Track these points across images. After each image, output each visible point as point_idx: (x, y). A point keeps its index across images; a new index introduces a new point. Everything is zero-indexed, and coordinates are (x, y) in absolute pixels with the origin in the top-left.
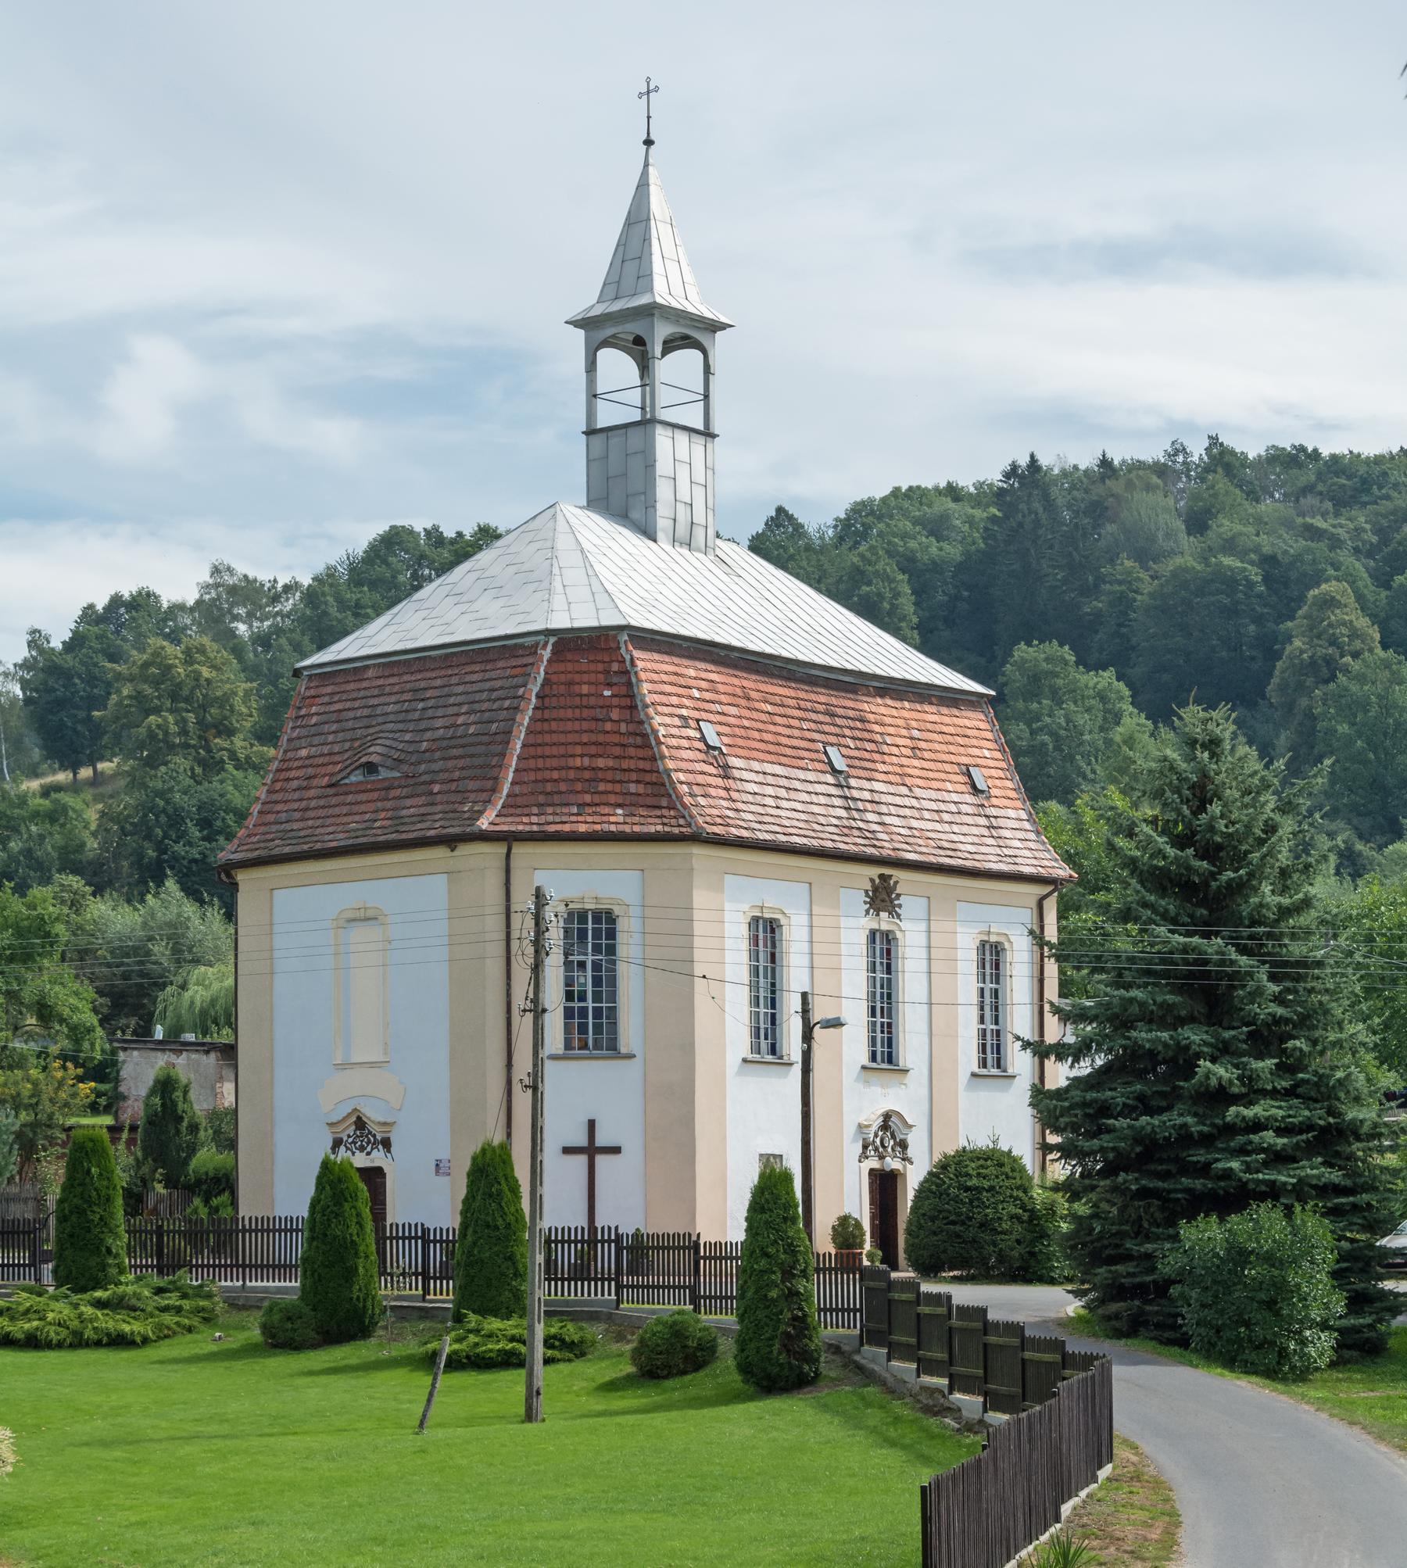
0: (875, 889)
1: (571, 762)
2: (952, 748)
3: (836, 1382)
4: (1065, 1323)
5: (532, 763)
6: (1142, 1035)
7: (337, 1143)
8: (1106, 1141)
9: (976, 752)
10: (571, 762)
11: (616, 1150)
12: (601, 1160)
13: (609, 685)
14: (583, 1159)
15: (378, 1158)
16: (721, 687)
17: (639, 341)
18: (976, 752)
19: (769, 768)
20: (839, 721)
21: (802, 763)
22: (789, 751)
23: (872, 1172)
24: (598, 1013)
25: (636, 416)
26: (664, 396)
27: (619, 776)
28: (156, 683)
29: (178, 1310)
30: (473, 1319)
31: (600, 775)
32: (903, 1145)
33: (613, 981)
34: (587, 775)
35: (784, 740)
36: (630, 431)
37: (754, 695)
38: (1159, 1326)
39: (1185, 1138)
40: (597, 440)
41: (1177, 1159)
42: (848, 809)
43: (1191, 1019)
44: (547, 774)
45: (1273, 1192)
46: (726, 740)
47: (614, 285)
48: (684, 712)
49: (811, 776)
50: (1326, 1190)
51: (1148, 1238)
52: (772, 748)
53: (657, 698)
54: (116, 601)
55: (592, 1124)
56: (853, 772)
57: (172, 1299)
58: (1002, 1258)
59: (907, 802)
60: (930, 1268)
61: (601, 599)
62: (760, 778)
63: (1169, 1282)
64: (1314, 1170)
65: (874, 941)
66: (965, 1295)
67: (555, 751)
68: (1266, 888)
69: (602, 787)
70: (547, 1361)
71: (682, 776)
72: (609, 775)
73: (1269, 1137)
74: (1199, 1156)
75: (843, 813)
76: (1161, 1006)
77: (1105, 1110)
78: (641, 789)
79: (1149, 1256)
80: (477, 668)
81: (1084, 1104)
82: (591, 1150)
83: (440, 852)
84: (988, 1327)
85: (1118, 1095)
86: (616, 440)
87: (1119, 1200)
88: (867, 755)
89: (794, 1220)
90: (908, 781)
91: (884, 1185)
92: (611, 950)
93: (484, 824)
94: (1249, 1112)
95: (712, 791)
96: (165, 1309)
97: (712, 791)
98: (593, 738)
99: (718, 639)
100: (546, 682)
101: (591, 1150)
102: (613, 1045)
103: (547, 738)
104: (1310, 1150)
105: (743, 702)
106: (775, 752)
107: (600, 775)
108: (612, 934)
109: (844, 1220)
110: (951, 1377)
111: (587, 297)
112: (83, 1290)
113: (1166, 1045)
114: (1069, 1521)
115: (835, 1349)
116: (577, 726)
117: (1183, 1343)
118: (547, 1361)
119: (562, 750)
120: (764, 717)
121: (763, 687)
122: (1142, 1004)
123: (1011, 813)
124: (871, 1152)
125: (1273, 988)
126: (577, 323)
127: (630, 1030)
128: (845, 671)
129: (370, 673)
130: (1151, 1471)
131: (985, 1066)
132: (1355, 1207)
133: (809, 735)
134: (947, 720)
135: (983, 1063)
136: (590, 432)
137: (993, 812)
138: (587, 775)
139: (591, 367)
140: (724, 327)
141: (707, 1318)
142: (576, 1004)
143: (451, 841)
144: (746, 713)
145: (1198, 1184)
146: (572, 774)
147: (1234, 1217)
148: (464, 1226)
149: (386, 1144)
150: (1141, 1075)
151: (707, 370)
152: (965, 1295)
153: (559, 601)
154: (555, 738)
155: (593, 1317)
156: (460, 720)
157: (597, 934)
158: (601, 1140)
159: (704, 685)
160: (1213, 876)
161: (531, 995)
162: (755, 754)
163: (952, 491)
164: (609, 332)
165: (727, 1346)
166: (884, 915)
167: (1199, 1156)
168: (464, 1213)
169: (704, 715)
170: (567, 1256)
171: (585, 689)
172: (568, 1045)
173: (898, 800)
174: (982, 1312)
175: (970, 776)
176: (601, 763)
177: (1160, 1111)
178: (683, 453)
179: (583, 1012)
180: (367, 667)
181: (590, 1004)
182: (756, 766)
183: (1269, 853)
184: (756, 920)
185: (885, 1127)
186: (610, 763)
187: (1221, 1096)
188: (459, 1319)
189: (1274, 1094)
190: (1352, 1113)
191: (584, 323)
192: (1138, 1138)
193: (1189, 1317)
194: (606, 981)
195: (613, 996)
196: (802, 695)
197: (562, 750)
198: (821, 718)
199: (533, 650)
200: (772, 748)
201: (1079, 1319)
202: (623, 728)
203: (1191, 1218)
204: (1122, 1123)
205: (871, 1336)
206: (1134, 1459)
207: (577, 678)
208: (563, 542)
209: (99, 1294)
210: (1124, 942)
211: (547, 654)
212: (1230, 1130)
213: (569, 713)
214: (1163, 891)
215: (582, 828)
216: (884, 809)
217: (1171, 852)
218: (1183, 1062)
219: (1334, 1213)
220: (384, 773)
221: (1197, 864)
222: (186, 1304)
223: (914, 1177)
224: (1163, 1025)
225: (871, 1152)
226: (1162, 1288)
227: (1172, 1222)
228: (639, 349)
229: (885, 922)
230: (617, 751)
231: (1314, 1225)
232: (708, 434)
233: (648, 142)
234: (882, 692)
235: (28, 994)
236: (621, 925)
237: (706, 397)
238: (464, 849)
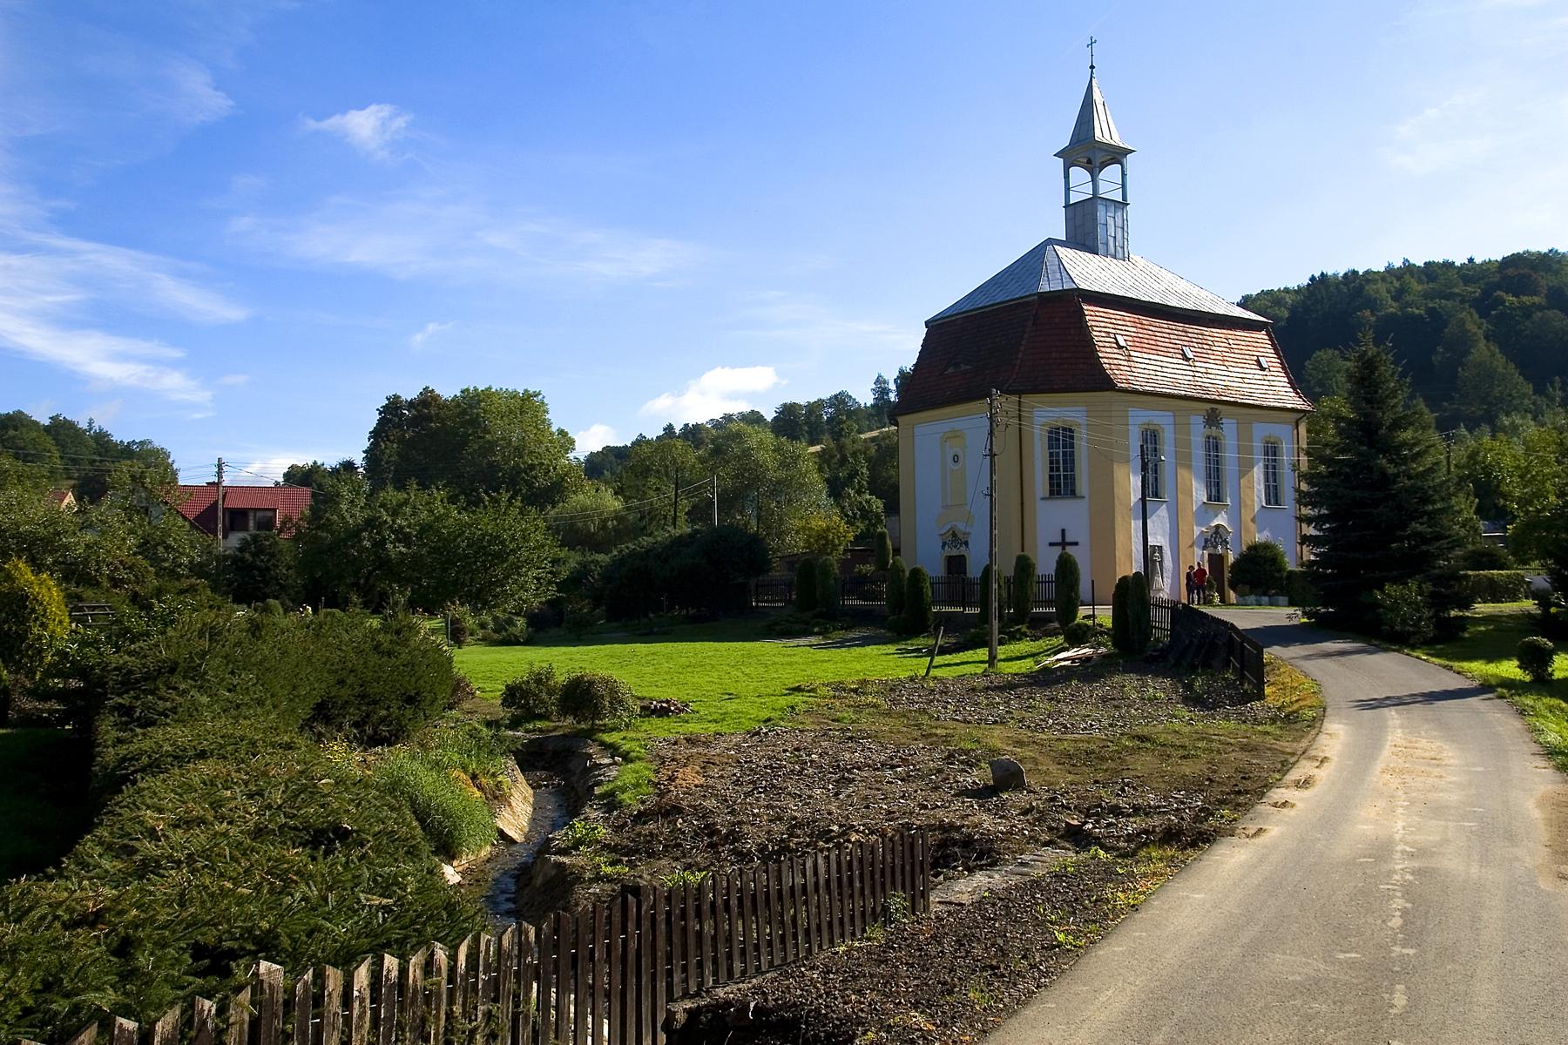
7: (944, 544)
16: (1127, 319)
21: (1170, 355)
33: (1073, 461)
36: (1085, 203)
46: (1129, 343)
53: (1094, 323)
55: (1063, 531)
56: (1196, 359)
71: (1106, 361)
90: (1226, 363)
95: (1122, 368)
97: (1122, 368)
105: (1139, 326)
127: (1082, 485)
131: (1270, 504)
135: (1268, 502)
149: (966, 543)
156: (998, 340)
158: (1068, 539)
161: (988, 447)
162: (1145, 350)
163: (1287, 290)
169: (1118, 332)
172: (1051, 493)
176: (1065, 355)
182: (1145, 356)
198: (1180, 333)
229: (1214, 431)
233: (1092, 67)
237: (1124, 186)
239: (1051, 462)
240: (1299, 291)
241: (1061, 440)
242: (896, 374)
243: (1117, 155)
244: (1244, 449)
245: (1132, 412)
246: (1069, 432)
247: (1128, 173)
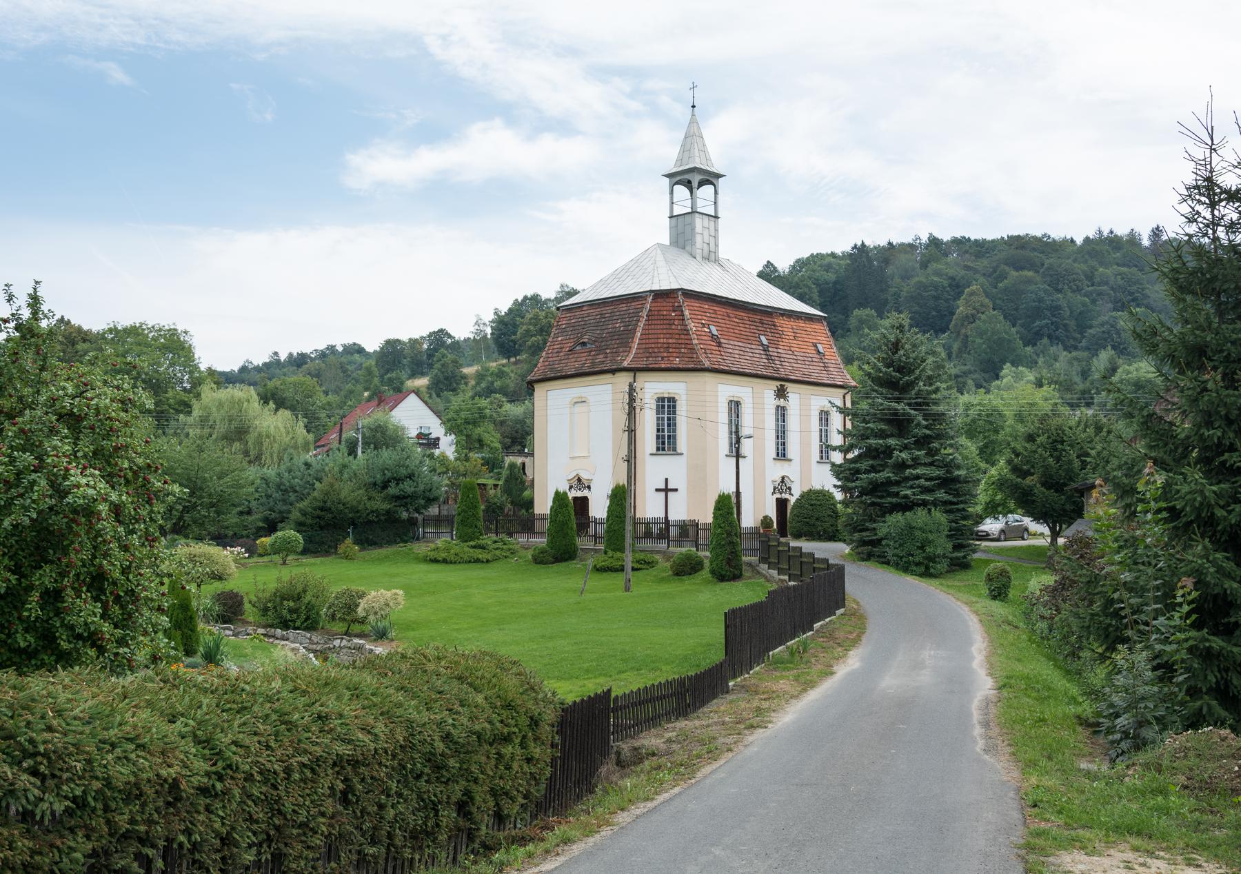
0: (778, 390)
3: (750, 578)
4: (843, 557)
6: (872, 441)
8: (858, 483)
11: (676, 490)
12: (670, 494)
13: (674, 311)
14: (663, 494)
15: (586, 493)
17: (689, 182)
19: (736, 343)
23: (777, 499)
24: (669, 437)
25: (690, 210)
26: (700, 203)
27: (678, 346)
28: (535, 325)
29: (502, 549)
30: (610, 553)
32: (790, 489)
33: (675, 425)
38: (878, 556)
39: (889, 482)
41: (886, 491)
43: (892, 436)
45: (924, 504)
47: (680, 160)
49: (753, 347)
50: (945, 503)
51: (875, 522)
54: (526, 298)
55: (667, 480)
57: (500, 545)
58: (825, 531)
60: (797, 536)
63: (882, 539)
64: (941, 495)
66: (794, 544)
68: (921, 383)
70: (633, 569)
73: (922, 481)
74: (895, 489)
76: (881, 430)
77: (858, 471)
78: (686, 351)
79: (874, 529)
81: (850, 469)
82: (666, 490)
83: (609, 376)
84: (802, 554)
85: (863, 465)
86: (680, 219)
87: (863, 506)
89: (732, 514)
91: (781, 504)
92: (674, 413)
93: (625, 364)
94: (914, 472)
96: (497, 549)
100: (650, 310)
101: (666, 490)
102: (675, 449)
104: (940, 486)
106: (740, 339)
108: (674, 407)
109: (766, 517)
110: (790, 575)
112: (466, 541)
113: (881, 445)
114: (817, 631)
115: (750, 564)
117: (888, 563)
118: (633, 569)
122: (872, 429)
124: (777, 491)
125: (924, 423)
126: (666, 176)
128: (768, 307)
129: (585, 308)
130: (862, 612)
132: (958, 510)
135: (822, 458)
139: (672, 192)
140: (722, 176)
141: (700, 553)
142: (661, 434)
143: (613, 372)
145: (894, 500)
147: (908, 513)
148: (608, 517)
149: (589, 487)
150: (874, 458)
151: (716, 193)
152: (807, 546)
153: (656, 280)
155: (658, 552)
157: (669, 407)
160: (901, 379)
163: (833, 255)
164: (678, 178)
165: (707, 563)
166: (782, 400)
167: (895, 489)
168: (608, 512)
170: (655, 530)
172: (658, 449)
174: (801, 548)
175: (816, 346)
176: (670, 341)
177: (879, 471)
178: (706, 224)
179: (664, 436)
181: (666, 434)
182: (732, 342)
183: (923, 370)
185: (782, 482)
186: (674, 341)
187: (902, 466)
188: (606, 553)
189: (925, 465)
190: (957, 473)
191: (669, 176)
192: (871, 483)
193: (890, 553)
194: (672, 424)
195: (675, 431)
199: (645, 298)
201: (849, 554)
203: (891, 513)
204: (865, 476)
205: (764, 560)
206: (856, 607)
209: (471, 543)
210: (864, 406)
211: (650, 299)
212: (907, 479)
213: (658, 322)
214: (881, 385)
215: (663, 366)
217: (884, 369)
218: (888, 452)
219: (946, 512)
221: (894, 374)
222: (505, 547)
223: (793, 500)
224: (881, 437)
225: (777, 491)
226: (879, 541)
227: (883, 515)
228: (688, 184)
229: (782, 402)
230: (677, 336)
231: (939, 516)
232: (716, 217)
233: (693, 107)
234: (783, 315)
235: (475, 437)
236: (678, 403)
238: (618, 375)
239: (658, 425)
240: (846, 256)
242: (492, 317)
243: (710, 178)
244: (804, 415)
245: (721, 387)
246: (672, 401)
247: (720, 191)
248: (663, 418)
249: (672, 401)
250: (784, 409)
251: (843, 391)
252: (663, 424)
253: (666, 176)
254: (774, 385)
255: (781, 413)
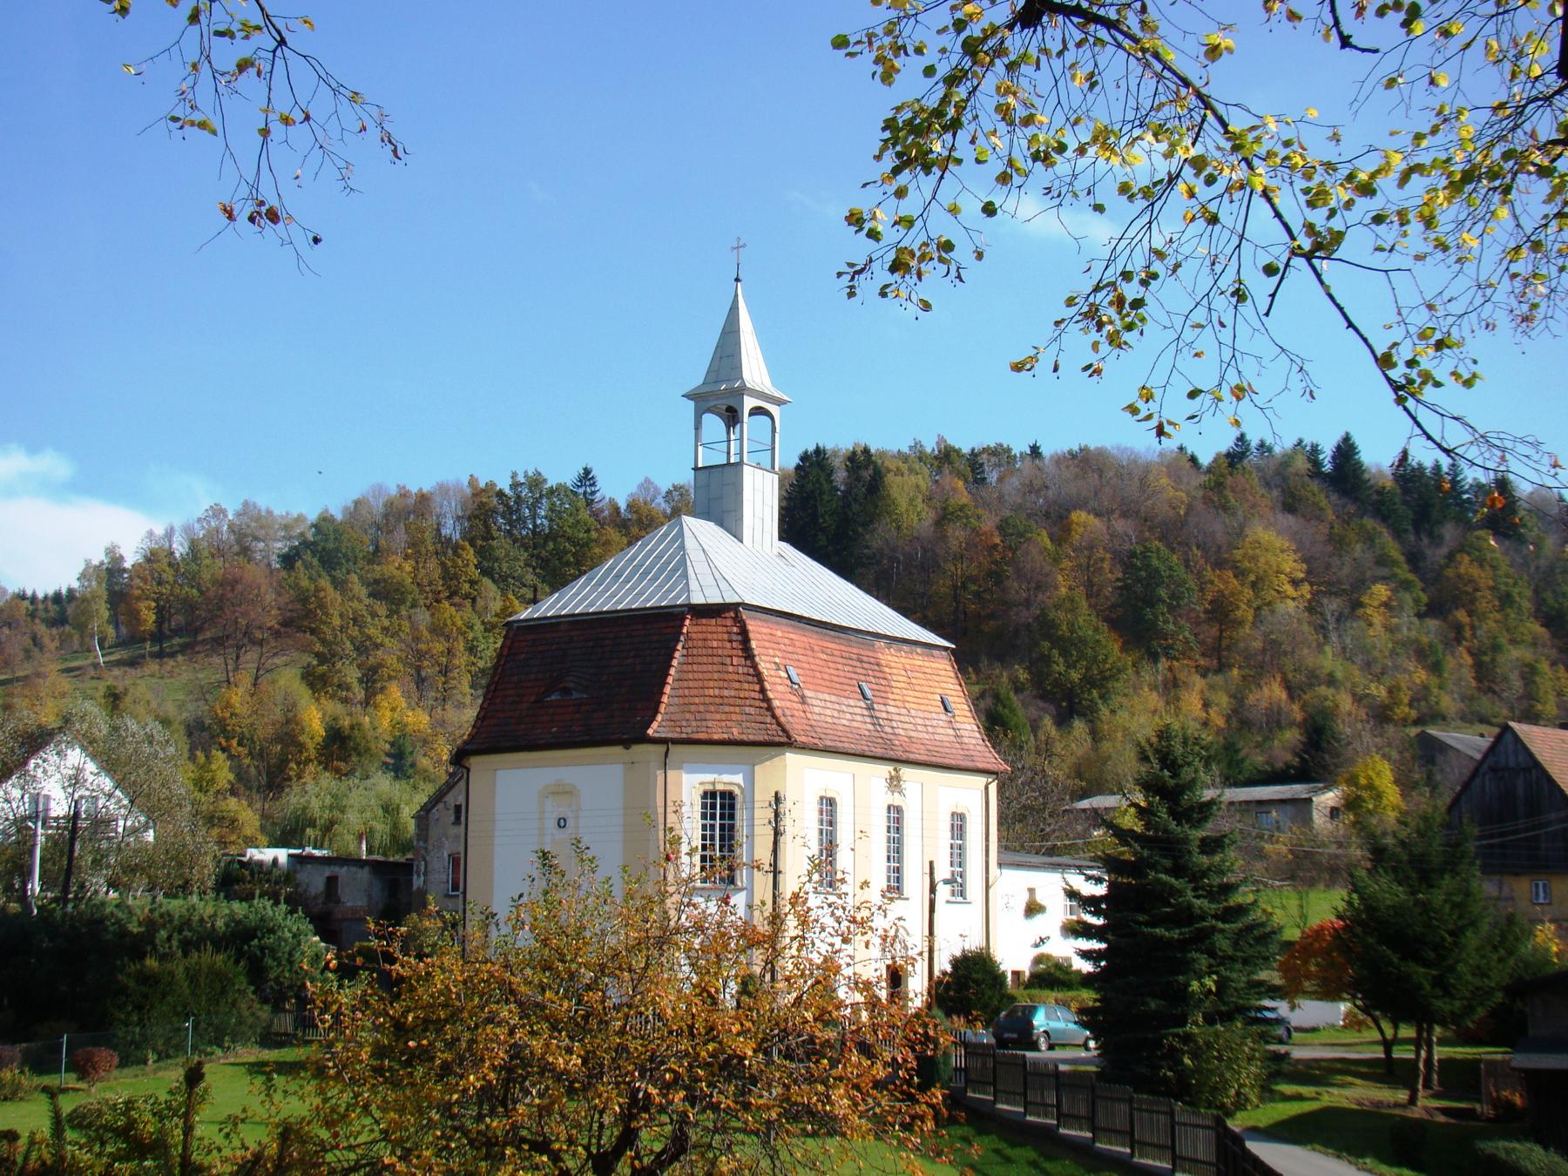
0: (891, 778)
1: (707, 692)
2: (931, 683)
5: (681, 692)
9: (945, 685)
10: (707, 692)
18: (945, 685)
20: (866, 665)
21: (846, 694)
22: (838, 686)
27: (739, 702)
31: (726, 700)
34: (718, 701)
35: (836, 679)
37: (816, 648)
40: (699, 472)
42: (874, 724)
44: (692, 700)
48: (777, 660)
49: (852, 702)
52: (828, 683)
56: (875, 700)
59: (907, 719)
61: (723, 584)
62: (823, 704)
65: (889, 812)
67: (697, 684)
69: (727, 709)
72: (732, 701)
75: (871, 727)
80: (640, 627)
88: (883, 688)
92: (732, 817)
95: (796, 713)
98: (721, 676)
99: (795, 612)
103: (690, 676)
107: (726, 700)
108: (732, 807)
111: (696, 379)
116: (710, 668)
119: (700, 684)
120: (822, 663)
121: (821, 643)
123: (968, 727)
126: (687, 396)
133: (848, 675)
134: (927, 664)
136: (696, 469)
137: (958, 726)
138: (718, 701)
142: (708, 853)
143: (626, 744)
144: (811, 660)
146: (707, 700)
153: (693, 585)
154: (696, 676)
157: (722, 807)
159: (787, 641)
162: (819, 688)
169: (788, 662)
171: (715, 644)
173: (902, 718)
176: (726, 693)
180: (559, 623)
184: (822, 798)
196: (843, 648)
197: (700, 684)
198: (855, 663)
200: (828, 683)
202: (741, 670)
207: (709, 636)
208: (690, 543)
216: (895, 725)
220: (576, 695)
229: (896, 800)
230: (737, 685)
241: (720, 806)
248: (712, 827)
249: (728, 798)
250: (899, 810)
251: (981, 781)
252: (712, 838)
253: (687, 396)
254: (885, 770)
255: (896, 817)
